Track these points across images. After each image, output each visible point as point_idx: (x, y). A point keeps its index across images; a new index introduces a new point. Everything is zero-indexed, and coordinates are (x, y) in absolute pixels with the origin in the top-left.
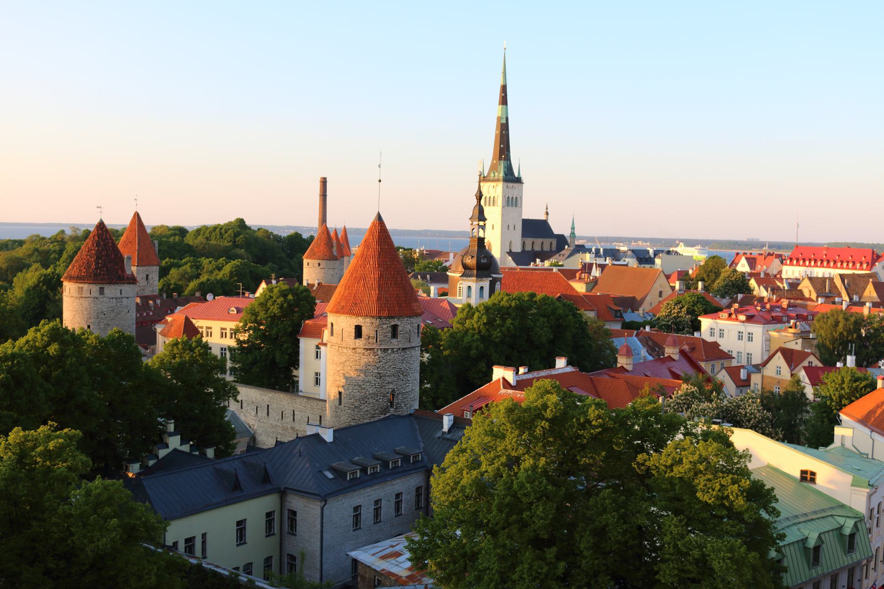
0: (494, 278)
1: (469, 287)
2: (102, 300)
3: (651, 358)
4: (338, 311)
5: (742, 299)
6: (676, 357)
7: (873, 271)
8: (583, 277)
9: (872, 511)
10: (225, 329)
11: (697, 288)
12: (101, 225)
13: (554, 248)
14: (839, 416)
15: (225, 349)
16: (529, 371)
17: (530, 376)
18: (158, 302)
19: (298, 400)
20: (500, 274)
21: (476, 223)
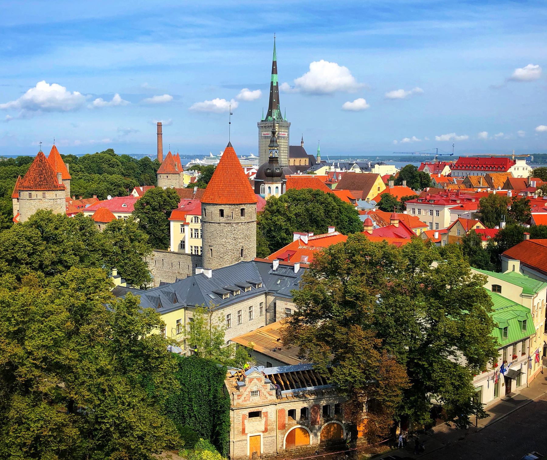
0: (284, 181)
1: (269, 188)
3: (378, 227)
5: (430, 190)
6: (397, 225)
7: (508, 171)
9: (534, 307)
11: (402, 185)
13: (307, 164)
14: (500, 257)
16: (314, 235)
17: (315, 238)
19: (181, 256)
20: (286, 179)
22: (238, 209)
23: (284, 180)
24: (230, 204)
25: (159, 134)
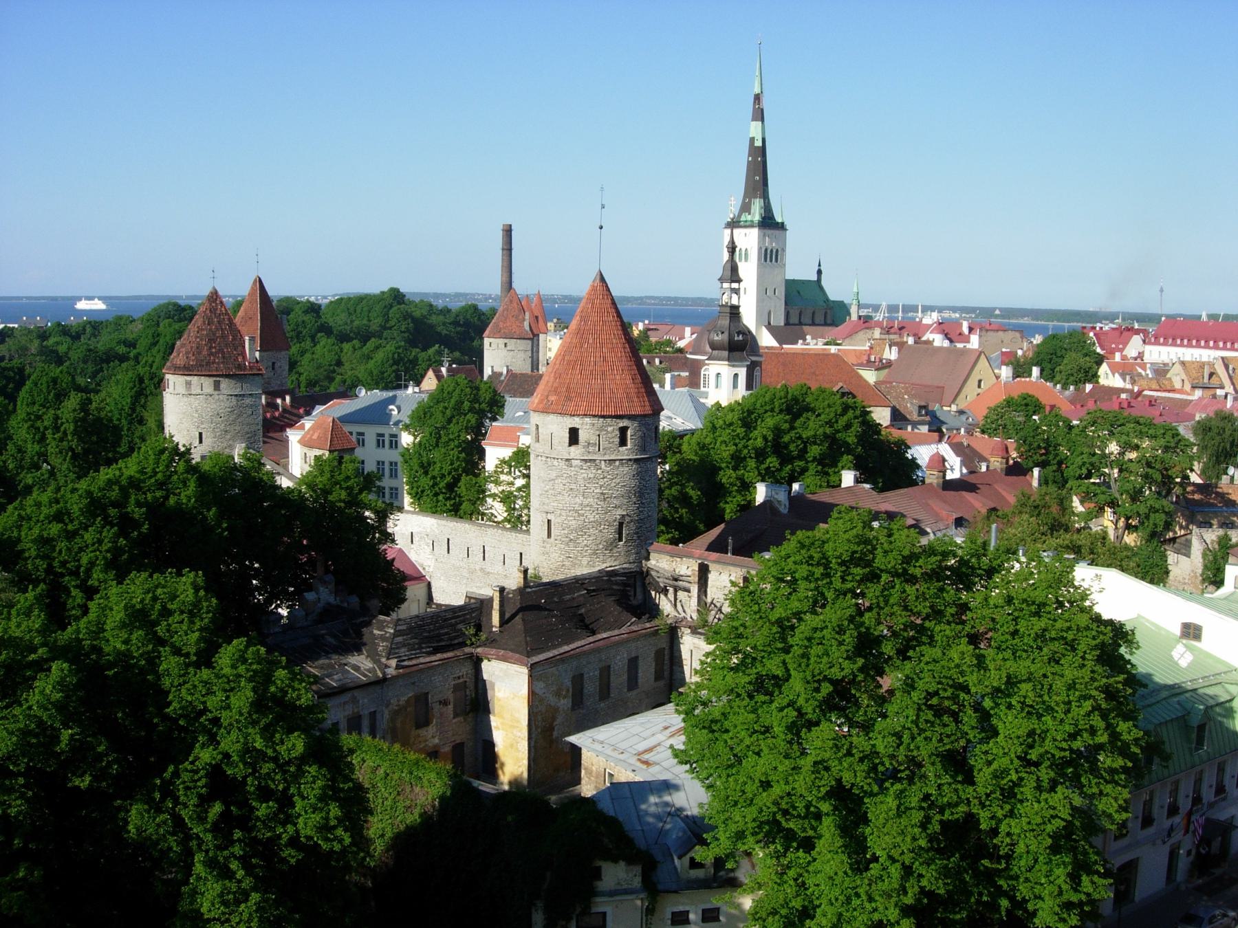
2: (217, 397)
4: (545, 410)
8: (873, 359)
10: (383, 435)
11: (1030, 375)
12: (214, 297)
15: (383, 463)
18: (288, 398)
20: (761, 356)
21: (726, 285)
22: (613, 427)
23: (754, 358)
24: (594, 416)
25: (508, 249)
